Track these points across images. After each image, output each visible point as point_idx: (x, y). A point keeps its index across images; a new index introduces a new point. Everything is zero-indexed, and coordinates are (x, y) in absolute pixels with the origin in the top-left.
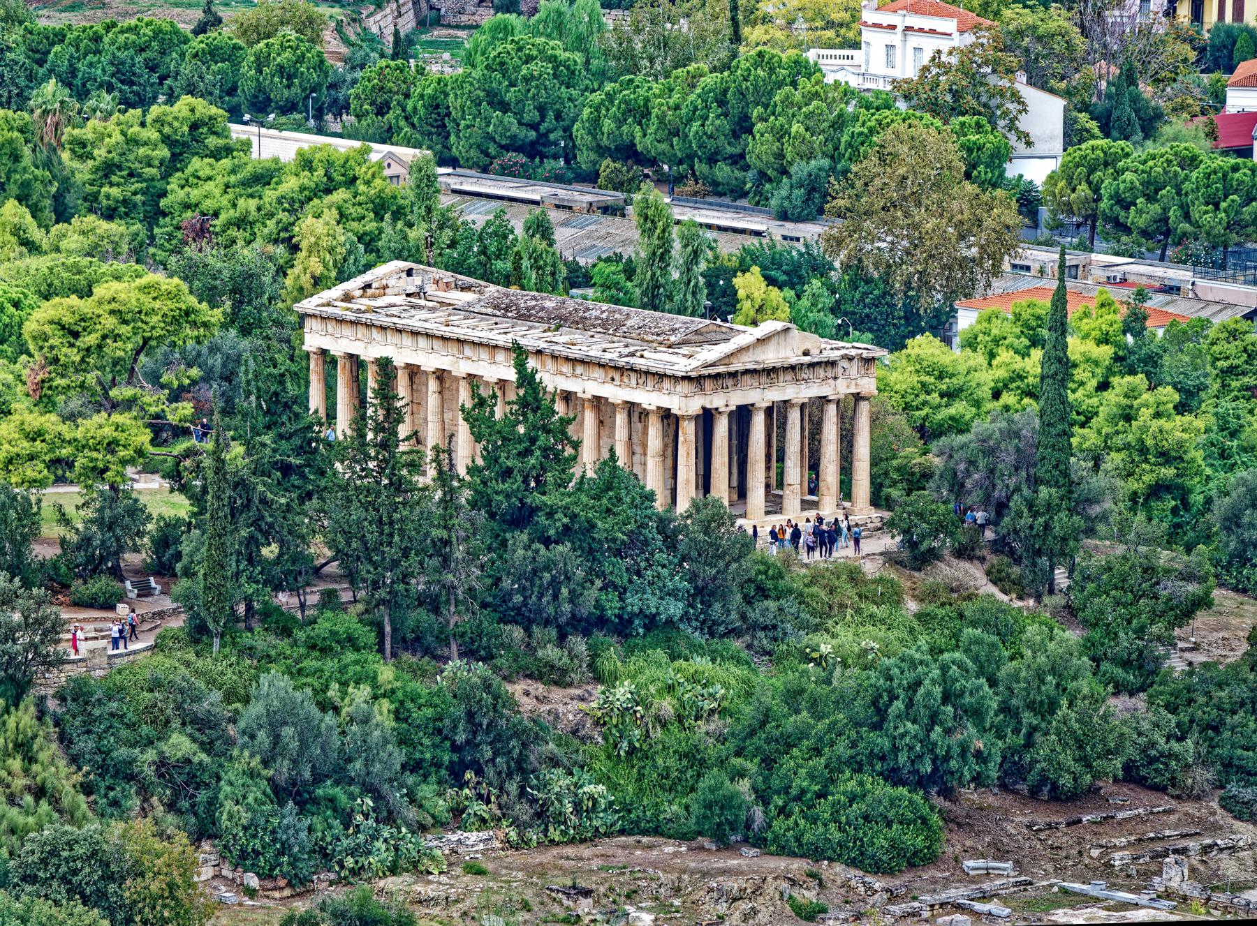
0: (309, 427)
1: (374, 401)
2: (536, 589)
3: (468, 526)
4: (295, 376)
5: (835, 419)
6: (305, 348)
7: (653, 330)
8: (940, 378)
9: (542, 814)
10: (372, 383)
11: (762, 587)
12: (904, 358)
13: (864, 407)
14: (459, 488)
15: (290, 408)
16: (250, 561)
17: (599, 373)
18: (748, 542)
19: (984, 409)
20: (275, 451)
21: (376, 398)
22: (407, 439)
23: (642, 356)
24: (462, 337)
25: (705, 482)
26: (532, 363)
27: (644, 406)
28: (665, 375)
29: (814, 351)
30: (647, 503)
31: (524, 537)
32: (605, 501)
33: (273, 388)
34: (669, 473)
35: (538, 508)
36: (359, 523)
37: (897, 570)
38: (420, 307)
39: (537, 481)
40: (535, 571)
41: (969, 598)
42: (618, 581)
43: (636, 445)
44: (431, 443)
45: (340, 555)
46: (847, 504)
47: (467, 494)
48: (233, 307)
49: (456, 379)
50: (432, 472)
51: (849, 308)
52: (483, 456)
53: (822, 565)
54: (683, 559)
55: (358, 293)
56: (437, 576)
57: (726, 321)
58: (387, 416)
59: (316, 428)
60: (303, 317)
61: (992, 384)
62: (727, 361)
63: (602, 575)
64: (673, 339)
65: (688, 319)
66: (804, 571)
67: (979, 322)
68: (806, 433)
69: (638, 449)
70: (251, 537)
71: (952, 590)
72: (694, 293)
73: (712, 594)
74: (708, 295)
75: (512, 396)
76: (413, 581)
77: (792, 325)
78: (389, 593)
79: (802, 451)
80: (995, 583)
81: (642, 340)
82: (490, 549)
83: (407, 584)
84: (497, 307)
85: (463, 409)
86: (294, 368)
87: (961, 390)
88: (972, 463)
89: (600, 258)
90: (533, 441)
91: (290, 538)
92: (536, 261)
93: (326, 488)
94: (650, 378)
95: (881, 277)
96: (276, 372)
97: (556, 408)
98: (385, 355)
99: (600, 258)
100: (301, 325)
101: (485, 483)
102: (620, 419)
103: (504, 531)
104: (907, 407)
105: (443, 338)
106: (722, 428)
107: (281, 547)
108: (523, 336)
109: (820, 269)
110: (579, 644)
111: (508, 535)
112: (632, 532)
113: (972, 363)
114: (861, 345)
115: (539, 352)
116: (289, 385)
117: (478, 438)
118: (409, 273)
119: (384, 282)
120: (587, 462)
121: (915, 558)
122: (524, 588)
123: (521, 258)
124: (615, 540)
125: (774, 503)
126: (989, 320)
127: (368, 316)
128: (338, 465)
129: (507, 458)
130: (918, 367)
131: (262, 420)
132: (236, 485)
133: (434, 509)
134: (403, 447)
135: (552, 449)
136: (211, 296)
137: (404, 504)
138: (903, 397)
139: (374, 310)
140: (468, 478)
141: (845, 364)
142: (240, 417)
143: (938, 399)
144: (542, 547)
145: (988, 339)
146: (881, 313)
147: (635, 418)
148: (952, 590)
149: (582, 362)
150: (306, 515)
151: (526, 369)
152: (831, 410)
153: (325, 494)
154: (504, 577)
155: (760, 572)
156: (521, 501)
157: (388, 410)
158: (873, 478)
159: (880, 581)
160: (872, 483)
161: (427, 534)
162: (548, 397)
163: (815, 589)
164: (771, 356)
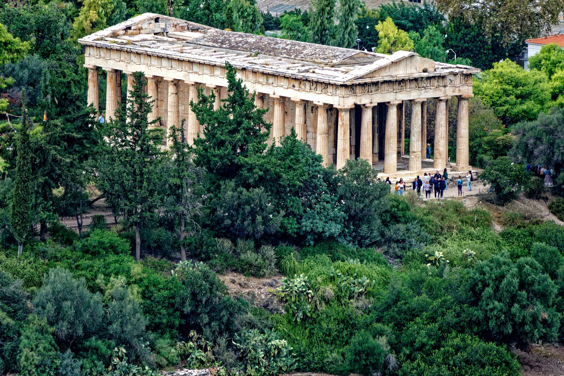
0: (87, 114)
1: (131, 99)
2: (240, 216)
3: (194, 176)
4: (77, 83)
5: (444, 112)
6: (85, 66)
7: (321, 56)
8: (516, 86)
9: (243, 359)
10: (130, 88)
11: (396, 214)
12: (491, 74)
13: (465, 105)
14: (188, 153)
15: (74, 103)
16: (45, 198)
17: (284, 83)
18: (385, 186)
19: (546, 105)
20: (63, 129)
21: (132, 97)
22: (154, 122)
23: (314, 72)
24: (192, 60)
25: (356, 149)
26: (238, 76)
27: (315, 103)
28: (330, 84)
29: (431, 70)
30: (316, 163)
31: (232, 184)
32: (288, 161)
33: (63, 91)
34: (332, 144)
35: (242, 166)
36: (120, 173)
37: (488, 205)
38: (164, 41)
39: (242, 148)
40: (239, 205)
41: (537, 223)
42: (296, 211)
43: (309, 126)
44: (170, 124)
45: (106, 194)
46: (453, 164)
47: (193, 157)
48: (37, 40)
49: (188, 86)
50: (170, 143)
51: (454, 43)
52: (205, 133)
53: (436, 202)
54: (341, 197)
55: (122, 32)
56: (172, 208)
57: (370, 50)
58: (140, 108)
59: (92, 116)
60: (84, 47)
61: (552, 90)
62: (371, 75)
63: (285, 207)
64: (334, 61)
65: (344, 49)
66: (424, 206)
67: (542, 52)
68: (425, 120)
69: (310, 129)
70: (46, 182)
71: (525, 218)
72: (349, 34)
73: (361, 220)
74: (359, 34)
75: (225, 96)
76: (156, 211)
77: (414, 54)
78: (139, 218)
79: (422, 131)
80: (554, 213)
81: (314, 62)
82: (209, 191)
83: (152, 212)
84: (215, 41)
85: (192, 104)
86: (77, 78)
87: (530, 94)
88: (538, 139)
89: (285, 12)
90: (239, 124)
91: (73, 183)
92: (242, 13)
93: (97, 152)
94: (319, 85)
95: (476, 25)
96: (65, 80)
97: (255, 103)
98: (139, 71)
99: (285, 12)
100: (83, 52)
101: (206, 150)
102: (299, 111)
103: (219, 180)
104: (494, 104)
105: (179, 60)
106: (367, 117)
107: (66, 189)
108: (233, 59)
109: (435, 19)
110: (269, 251)
111: (222, 183)
112: (306, 180)
113: (537, 77)
114: (463, 67)
115: (244, 69)
116: (73, 89)
117: (202, 122)
118: (157, 20)
119: (140, 26)
120: (276, 137)
121: (499, 198)
122: (232, 215)
123: (232, 12)
124: (294, 186)
125: (403, 163)
126: (549, 51)
127: (128, 46)
128: (106, 139)
129: (221, 135)
130: (501, 80)
131: (54, 110)
132: (36, 150)
133: (171, 166)
134: (150, 127)
135: (252, 129)
136: (22, 34)
137: (151, 163)
138: (491, 98)
139: (132, 43)
140: (194, 147)
141: (452, 77)
142: (40, 108)
143: (515, 99)
144: (245, 190)
145: (548, 62)
146: (476, 47)
147: (309, 110)
148: (525, 218)
149: (273, 75)
150: (84, 169)
151: (235, 80)
152: (442, 107)
153: (97, 156)
154: (218, 209)
155: (394, 206)
156: (230, 161)
157: (141, 104)
158: (471, 148)
159: (475, 212)
160: (470, 151)
161: (166, 182)
162: (250, 97)
163: (431, 217)
164: (401, 73)
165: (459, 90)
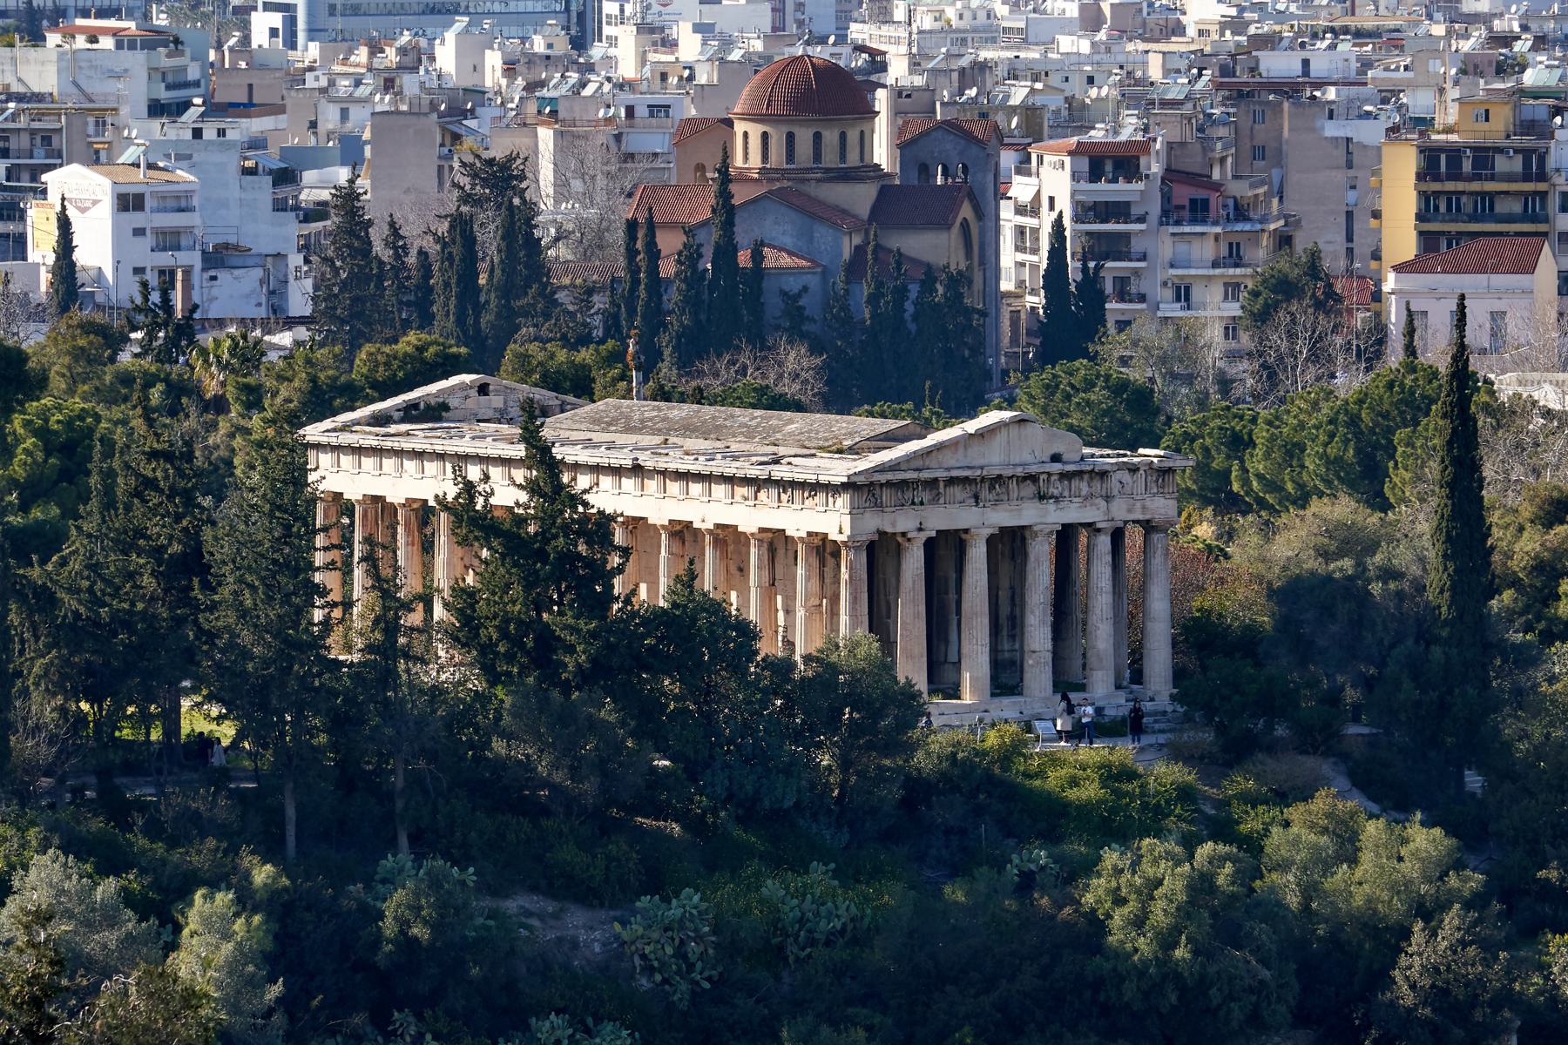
141: (1126, 476)
164: (994, 458)
165: (1144, 507)
